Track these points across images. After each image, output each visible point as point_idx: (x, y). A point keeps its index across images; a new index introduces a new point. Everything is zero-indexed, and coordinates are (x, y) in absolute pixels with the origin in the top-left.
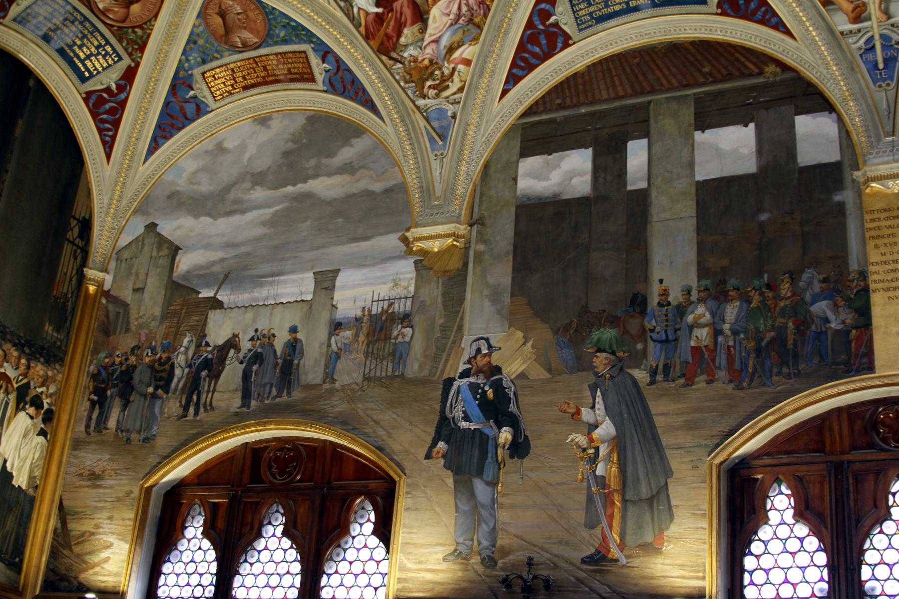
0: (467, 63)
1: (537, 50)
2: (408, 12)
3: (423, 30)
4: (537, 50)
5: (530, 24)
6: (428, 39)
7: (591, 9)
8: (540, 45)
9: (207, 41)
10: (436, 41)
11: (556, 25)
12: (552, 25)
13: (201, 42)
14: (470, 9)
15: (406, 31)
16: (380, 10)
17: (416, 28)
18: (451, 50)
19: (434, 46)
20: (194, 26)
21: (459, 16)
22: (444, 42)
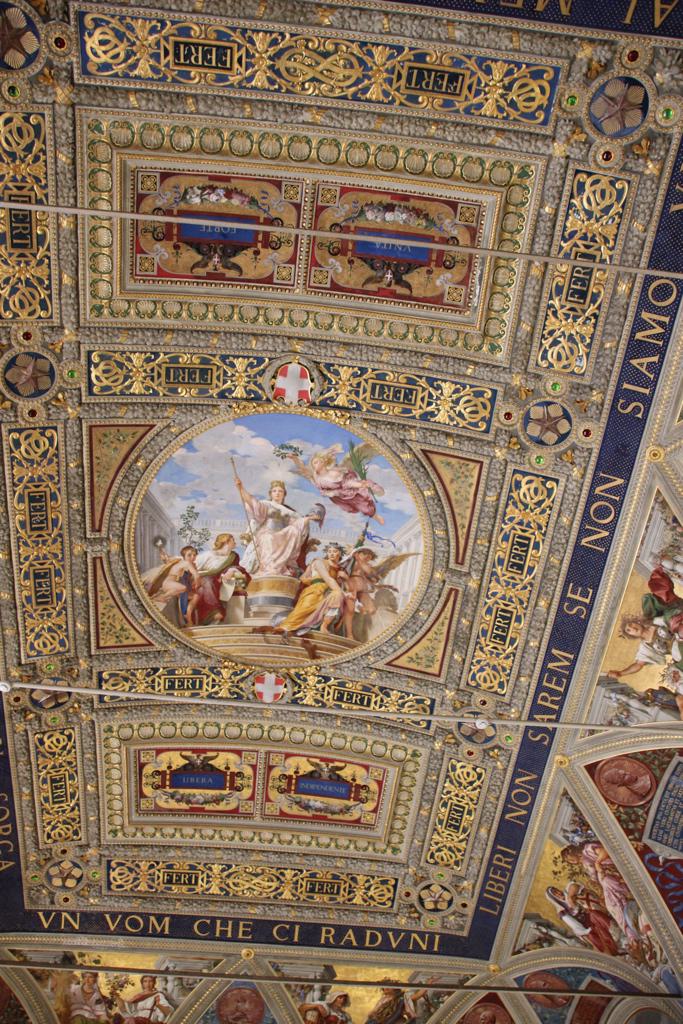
0: (648, 928)
1: (673, 885)
2: (600, 919)
3: (616, 924)
4: (673, 885)
5: (653, 875)
6: (622, 927)
7: (672, 834)
8: (672, 881)
9: (550, 1013)
10: (627, 926)
11: (666, 861)
12: (664, 863)
13: (548, 1016)
14: (620, 892)
15: (611, 931)
16: (589, 930)
17: (612, 926)
18: (636, 925)
19: (628, 930)
20: (536, 1010)
21: (620, 901)
22: (630, 923)
